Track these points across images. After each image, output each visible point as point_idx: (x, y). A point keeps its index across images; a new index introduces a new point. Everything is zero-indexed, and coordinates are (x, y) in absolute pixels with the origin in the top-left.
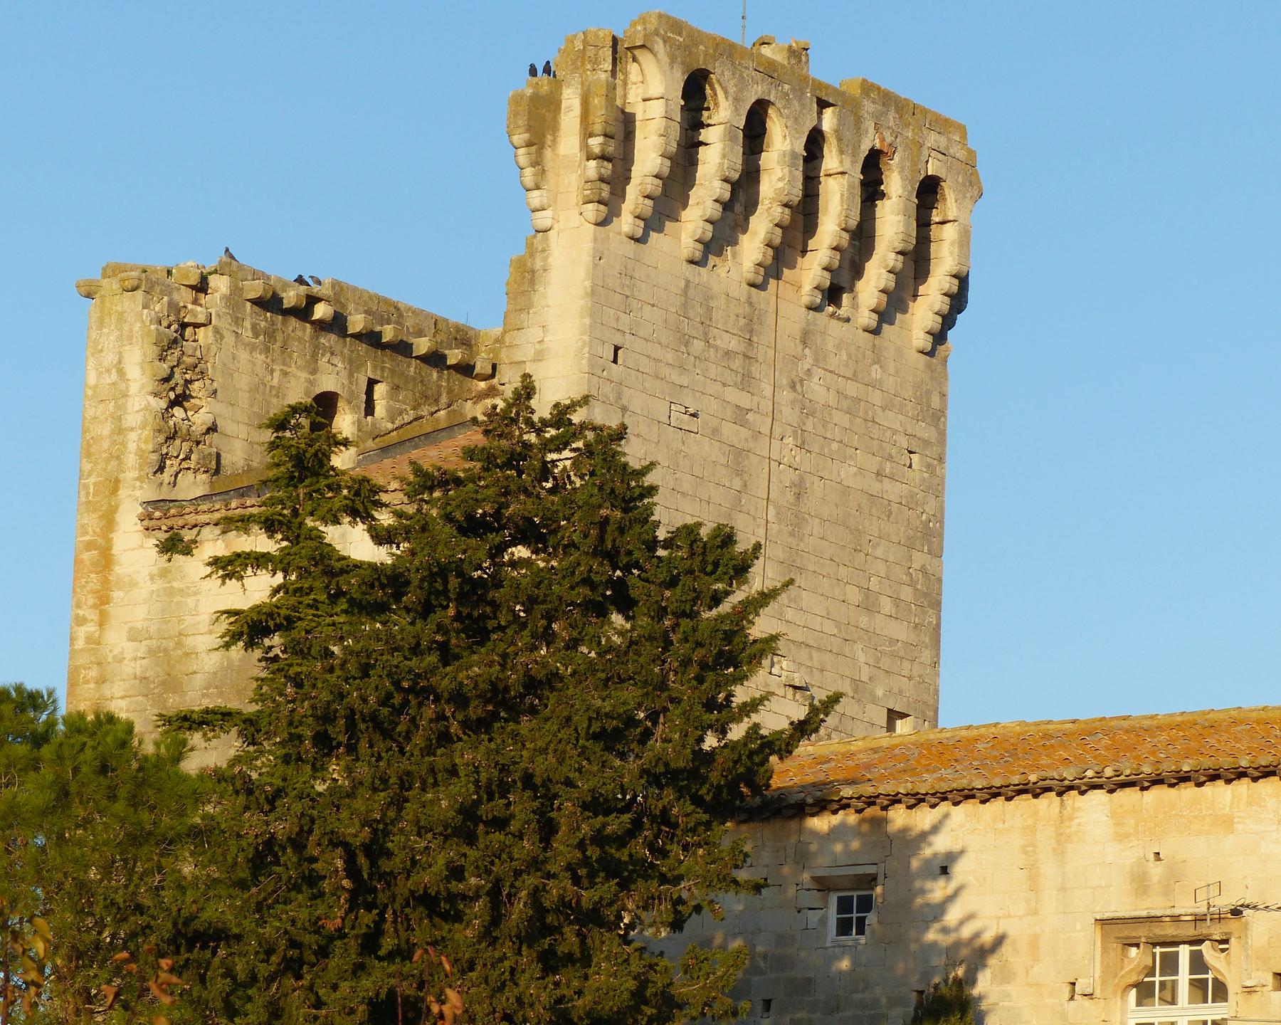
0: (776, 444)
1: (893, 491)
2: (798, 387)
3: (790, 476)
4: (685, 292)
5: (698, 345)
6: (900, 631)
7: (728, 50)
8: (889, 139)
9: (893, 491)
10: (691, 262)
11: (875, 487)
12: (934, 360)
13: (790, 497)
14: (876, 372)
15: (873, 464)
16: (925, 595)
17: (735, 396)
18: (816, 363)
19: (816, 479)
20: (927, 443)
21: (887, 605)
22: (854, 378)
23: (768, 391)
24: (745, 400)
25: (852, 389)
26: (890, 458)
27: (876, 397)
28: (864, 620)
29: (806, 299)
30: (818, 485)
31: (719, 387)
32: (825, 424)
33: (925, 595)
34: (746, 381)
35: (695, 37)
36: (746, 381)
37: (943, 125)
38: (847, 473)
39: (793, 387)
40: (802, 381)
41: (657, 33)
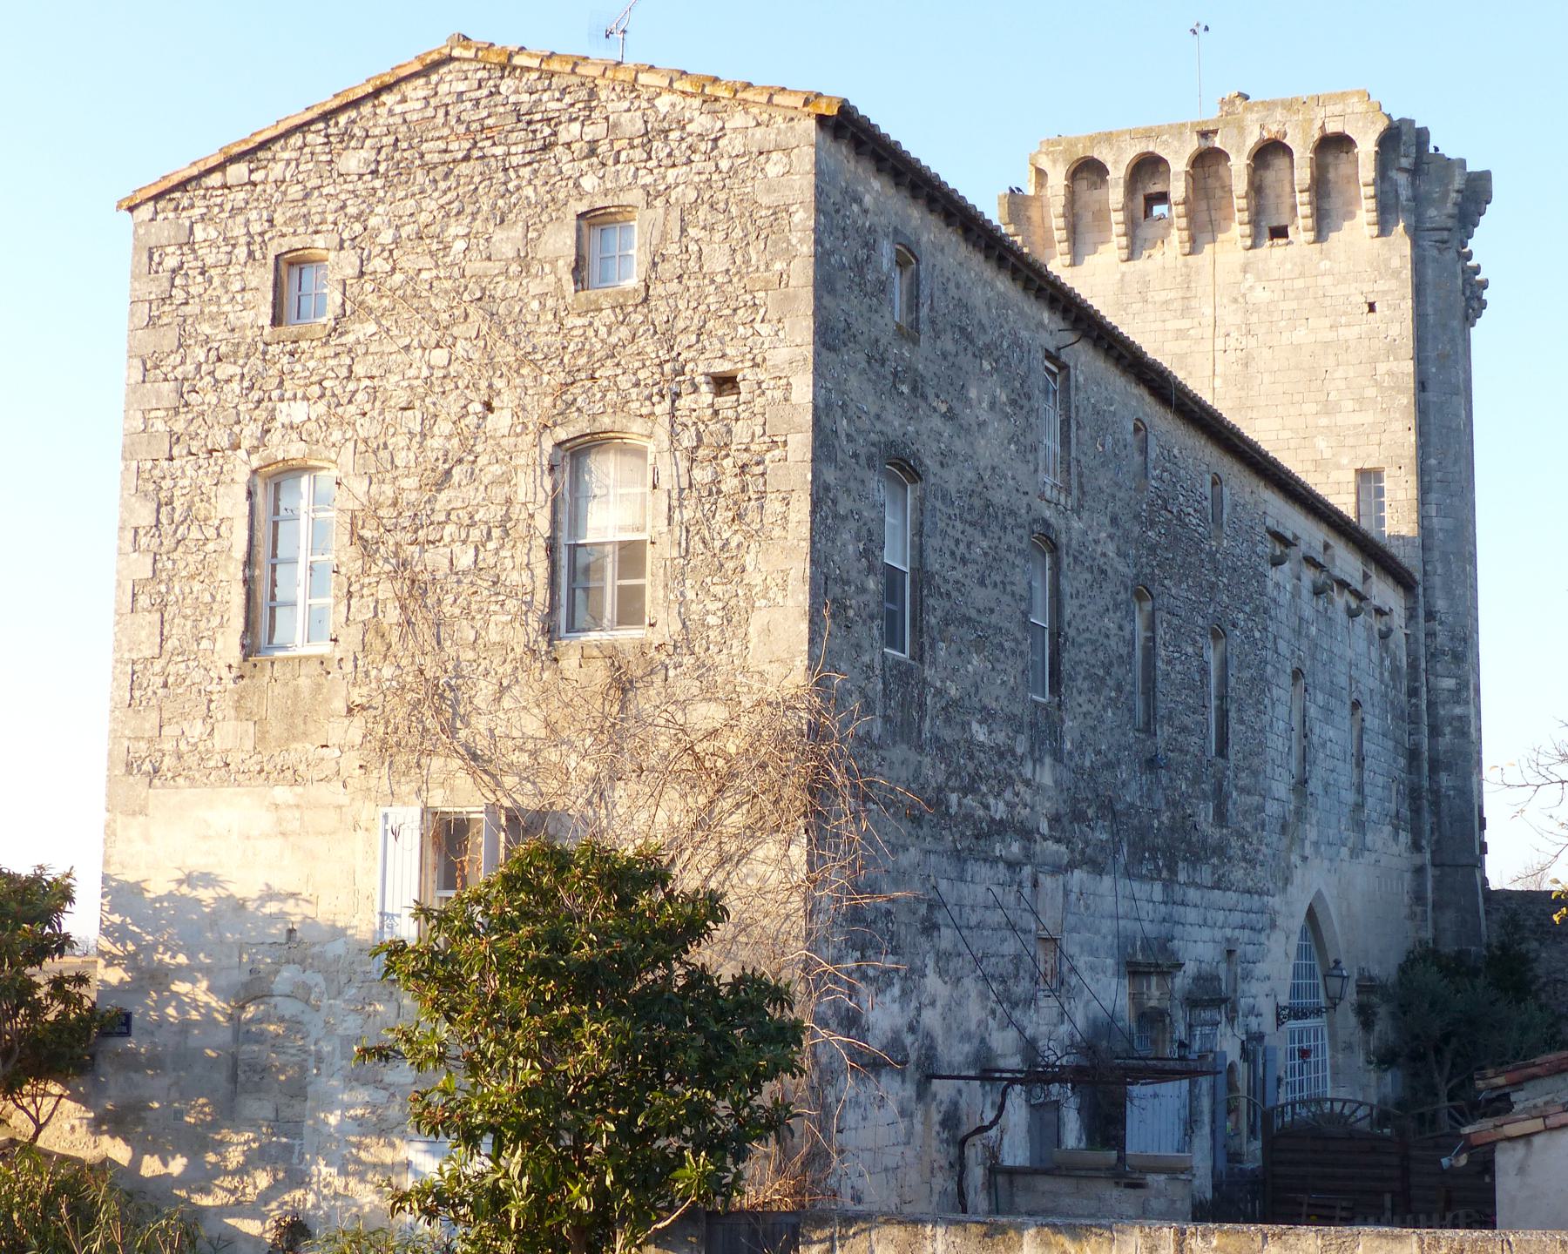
1: (1350, 333)
2: (1241, 300)
3: (1232, 356)
4: (1122, 280)
5: (1136, 307)
6: (1367, 417)
7: (1108, 138)
9: (1350, 333)
11: (1331, 336)
12: (1391, 238)
13: (1237, 368)
14: (1325, 265)
15: (1327, 322)
16: (1392, 388)
17: (1174, 324)
18: (1259, 279)
19: (1265, 351)
20: (1385, 293)
21: (1349, 405)
22: (1302, 275)
23: (1209, 311)
24: (1184, 324)
25: (1299, 283)
26: (1345, 313)
27: (1327, 280)
28: (1324, 421)
29: (1240, 245)
30: (1266, 353)
31: (1159, 324)
32: (1270, 313)
33: (1392, 388)
34: (1186, 311)
35: (1072, 144)
36: (1186, 311)
37: (1343, 96)
38: (1301, 335)
39: (1235, 300)
40: (1244, 296)
41: (1040, 152)
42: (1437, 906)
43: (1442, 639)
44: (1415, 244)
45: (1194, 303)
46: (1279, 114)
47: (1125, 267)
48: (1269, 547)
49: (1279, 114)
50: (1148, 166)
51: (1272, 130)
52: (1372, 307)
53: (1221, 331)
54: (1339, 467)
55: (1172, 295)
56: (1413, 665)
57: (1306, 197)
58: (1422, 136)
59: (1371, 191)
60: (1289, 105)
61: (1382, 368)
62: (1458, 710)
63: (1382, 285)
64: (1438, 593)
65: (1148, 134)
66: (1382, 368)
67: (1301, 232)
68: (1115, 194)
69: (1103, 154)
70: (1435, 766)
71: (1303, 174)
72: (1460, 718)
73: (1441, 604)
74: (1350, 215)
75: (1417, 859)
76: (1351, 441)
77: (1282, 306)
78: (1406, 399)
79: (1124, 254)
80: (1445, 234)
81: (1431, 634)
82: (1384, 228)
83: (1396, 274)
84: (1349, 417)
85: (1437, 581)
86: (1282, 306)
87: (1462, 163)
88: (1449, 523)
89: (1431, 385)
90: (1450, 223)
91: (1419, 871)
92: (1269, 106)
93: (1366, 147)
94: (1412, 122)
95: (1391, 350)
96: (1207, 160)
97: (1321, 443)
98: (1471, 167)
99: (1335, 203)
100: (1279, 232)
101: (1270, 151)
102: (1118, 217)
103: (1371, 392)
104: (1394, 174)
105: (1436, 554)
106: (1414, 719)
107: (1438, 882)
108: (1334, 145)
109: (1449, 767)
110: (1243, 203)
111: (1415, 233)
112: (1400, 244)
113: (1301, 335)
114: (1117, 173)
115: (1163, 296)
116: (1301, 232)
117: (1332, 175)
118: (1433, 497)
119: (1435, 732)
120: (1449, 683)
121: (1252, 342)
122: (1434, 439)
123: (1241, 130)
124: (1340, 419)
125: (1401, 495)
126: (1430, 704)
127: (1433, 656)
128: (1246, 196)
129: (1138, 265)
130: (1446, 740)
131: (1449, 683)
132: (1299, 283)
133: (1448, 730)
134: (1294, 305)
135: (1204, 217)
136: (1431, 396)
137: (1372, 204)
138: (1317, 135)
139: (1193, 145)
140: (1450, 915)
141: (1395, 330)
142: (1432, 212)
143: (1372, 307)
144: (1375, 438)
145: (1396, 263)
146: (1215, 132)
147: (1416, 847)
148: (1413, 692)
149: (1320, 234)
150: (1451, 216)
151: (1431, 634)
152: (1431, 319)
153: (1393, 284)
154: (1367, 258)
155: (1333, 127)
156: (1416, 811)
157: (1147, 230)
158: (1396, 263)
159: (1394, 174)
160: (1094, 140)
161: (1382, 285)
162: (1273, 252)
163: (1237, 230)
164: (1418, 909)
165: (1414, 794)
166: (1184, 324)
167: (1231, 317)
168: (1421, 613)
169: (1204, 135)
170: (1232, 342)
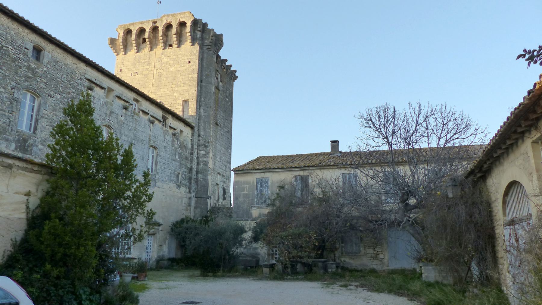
0: (155, 72)
6: (186, 88)
7: (133, 24)
8: (169, 20)
9: (184, 68)
10: (137, 53)
11: (180, 69)
14: (180, 53)
15: (179, 66)
18: (165, 56)
21: (182, 85)
23: (153, 64)
25: (174, 57)
27: (180, 56)
28: (176, 89)
34: (148, 64)
35: (125, 26)
38: (173, 69)
42: (195, 208)
43: (202, 142)
44: (200, 48)
45: (150, 62)
46: (170, 17)
47: (136, 54)
48: (87, 83)
49: (170, 17)
50: (142, 31)
51: (169, 21)
52: (189, 62)
53: (156, 69)
54: (179, 100)
55: (146, 61)
56: (192, 147)
57: (175, 36)
58: (205, 25)
59: (189, 34)
60: (173, 15)
61: (190, 76)
62: (205, 159)
63: (192, 57)
64: (201, 130)
65: (142, 23)
66: (190, 76)
67: (175, 46)
68: (134, 37)
69: (131, 28)
70: (197, 172)
71: (174, 30)
72: (206, 161)
73: (202, 133)
74: (186, 41)
75: (189, 195)
76: (182, 93)
77: (170, 62)
78: (195, 83)
79: (136, 51)
80: (209, 47)
81: (199, 140)
82: (193, 45)
83: (195, 54)
84: (182, 88)
85: (201, 127)
86: (170, 62)
87: (213, 30)
88: (206, 114)
89: (203, 81)
90: (210, 44)
91: (190, 198)
92: (168, 15)
93: (189, 24)
94: (201, 20)
95: (193, 72)
96: (155, 29)
97: (175, 94)
98: (218, 33)
99: (183, 38)
100: (171, 46)
101: (169, 27)
102: (134, 42)
103: (187, 82)
104: (197, 32)
105: (202, 121)
106: (192, 160)
107: (196, 203)
108: (182, 24)
109: (201, 173)
110: (161, 38)
111: (201, 47)
112: (197, 47)
113: (173, 69)
114: (134, 32)
115: (144, 61)
116: (175, 46)
117: (183, 32)
118: (202, 107)
119: (198, 164)
120: (203, 152)
121: (162, 71)
122: (203, 94)
123: (162, 21)
124: (180, 88)
125: (192, 106)
126: (198, 158)
127: (199, 146)
128: (162, 36)
129: (139, 54)
130: (201, 166)
131: (203, 152)
132: (174, 57)
133: (202, 164)
134: (172, 62)
135: (154, 43)
136: (203, 84)
137: (189, 37)
138: (178, 21)
139: (151, 25)
140: (198, 210)
141: (194, 67)
142: (206, 41)
143: (189, 62)
144: (187, 93)
145: (195, 52)
146: (156, 22)
147: (190, 192)
148: (192, 154)
149: (179, 46)
150: (211, 42)
151: (199, 140)
152: (205, 66)
153: (194, 57)
154: (190, 51)
155: (182, 20)
156: (190, 183)
157: (142, 46)
158: (195, 52)
159: (197, 32)
160: (130, 25)
161: (192, 57)
162: (169, 50)
163: (161, 46)
164: (189, 208)
165: (190, 179)
166: (148, 67)
167: (158, 65)
168: (196, 135)
169: (155, 23)
170: (158, 71)
